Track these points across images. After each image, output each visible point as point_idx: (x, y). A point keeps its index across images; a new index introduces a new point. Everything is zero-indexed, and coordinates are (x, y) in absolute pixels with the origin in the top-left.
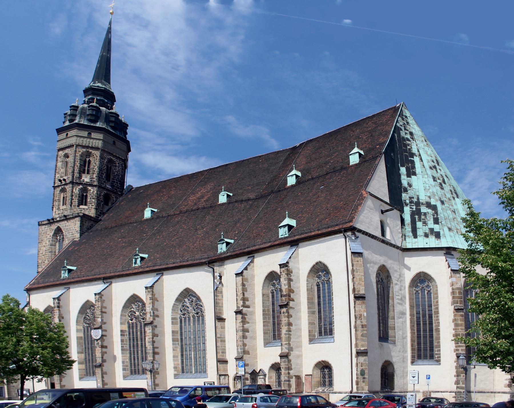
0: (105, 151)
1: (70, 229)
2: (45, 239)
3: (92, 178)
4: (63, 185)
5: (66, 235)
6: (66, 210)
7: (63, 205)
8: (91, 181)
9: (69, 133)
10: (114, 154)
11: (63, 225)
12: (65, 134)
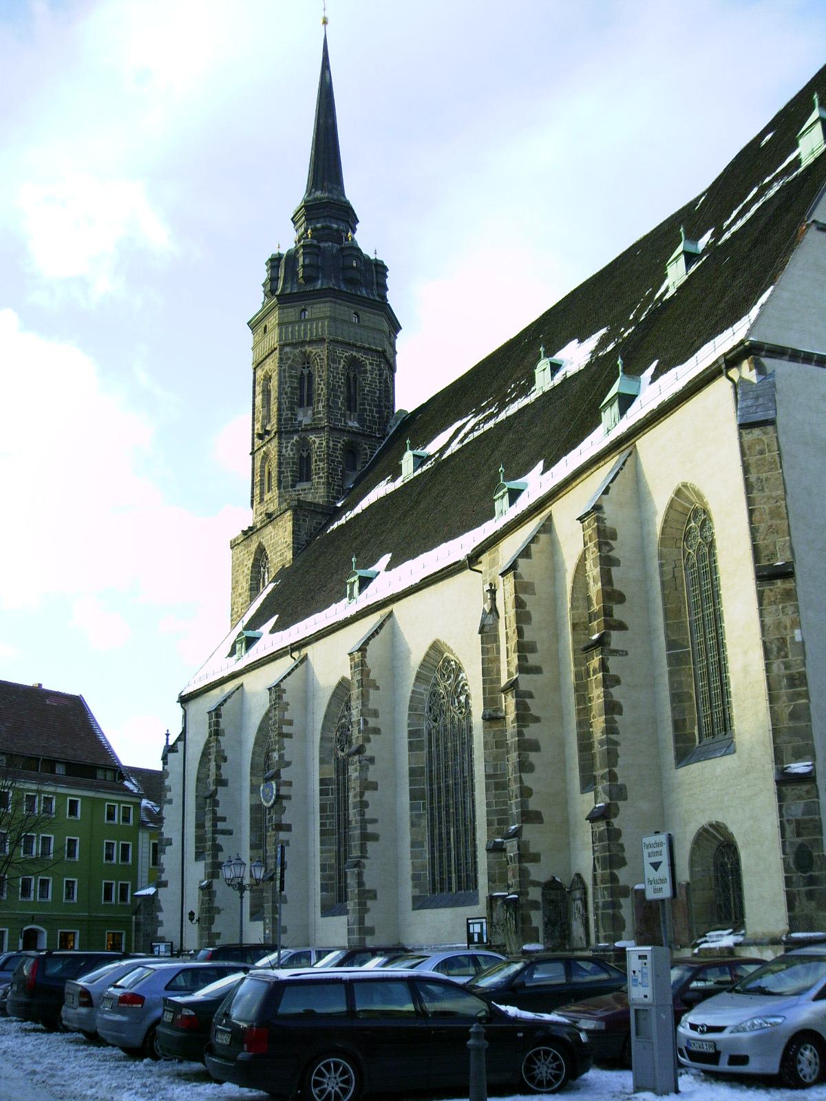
0: (337, 342)
2: (241, 577)
8: (314, 420)
10: (359, 344)
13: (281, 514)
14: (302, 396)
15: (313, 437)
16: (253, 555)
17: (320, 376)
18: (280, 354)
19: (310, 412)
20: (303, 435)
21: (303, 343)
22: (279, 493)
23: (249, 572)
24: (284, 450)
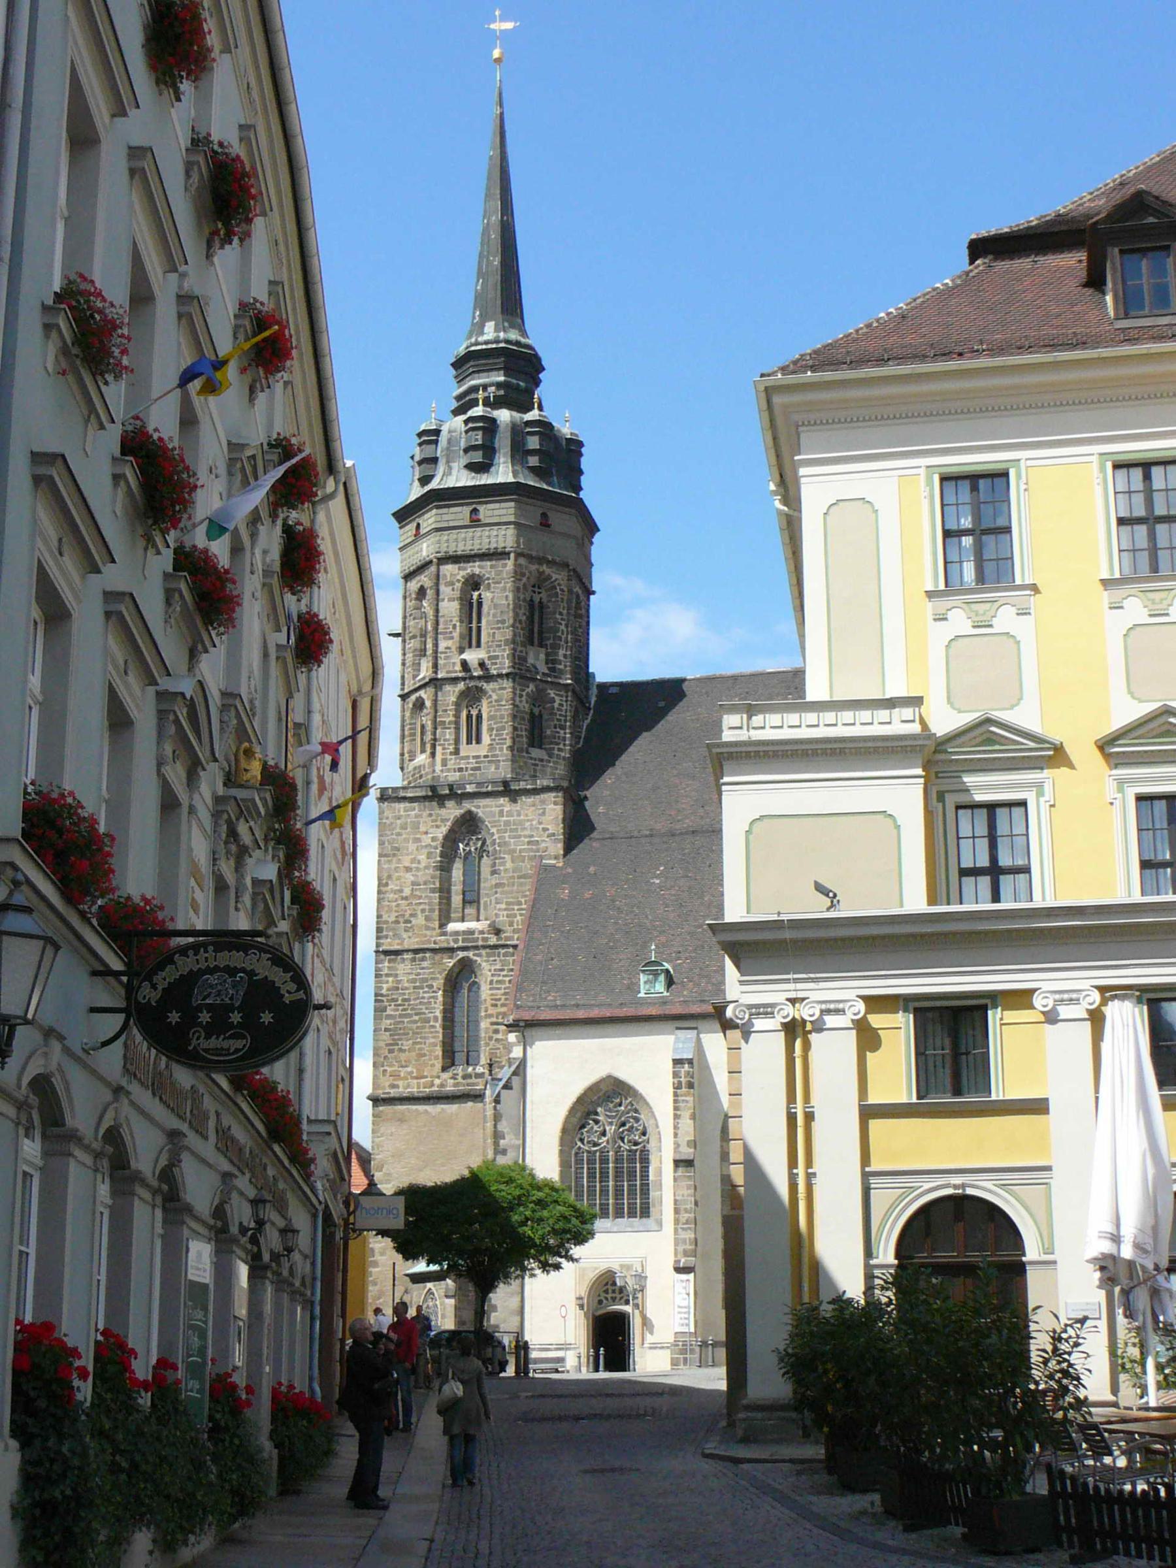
1: (521, 823)
3: (551, 661)
4: (472, 678)
5: (504, 844)
6: (492, 759)
7: (469, 742)
8: (553, 670)
9: (481, 508)
11: (484, 808)
12: (466, 510)
13: (534, 789)
14: (532, 631)
15: (552, 693)
16: (449, 823)
17: (561, 614)
18: (515, 565)
19: (542, 656)
20: (541, 686)
21: (541, 560)
22: (513, 755)
23: (438, 843)
24: (518, 699)
